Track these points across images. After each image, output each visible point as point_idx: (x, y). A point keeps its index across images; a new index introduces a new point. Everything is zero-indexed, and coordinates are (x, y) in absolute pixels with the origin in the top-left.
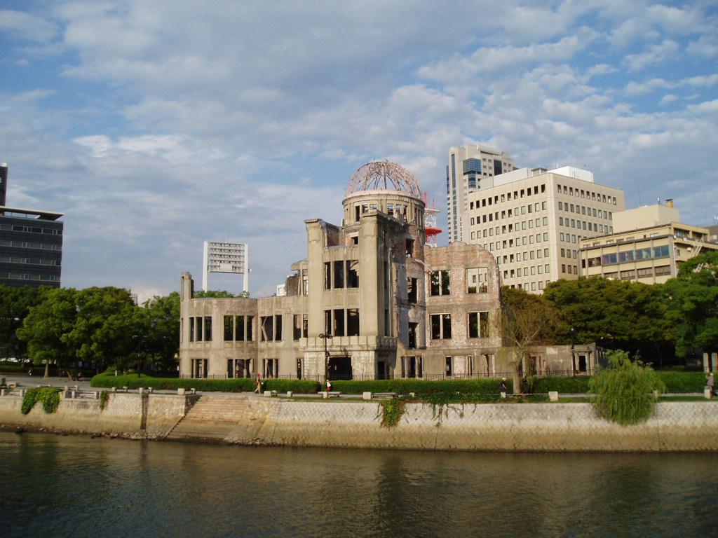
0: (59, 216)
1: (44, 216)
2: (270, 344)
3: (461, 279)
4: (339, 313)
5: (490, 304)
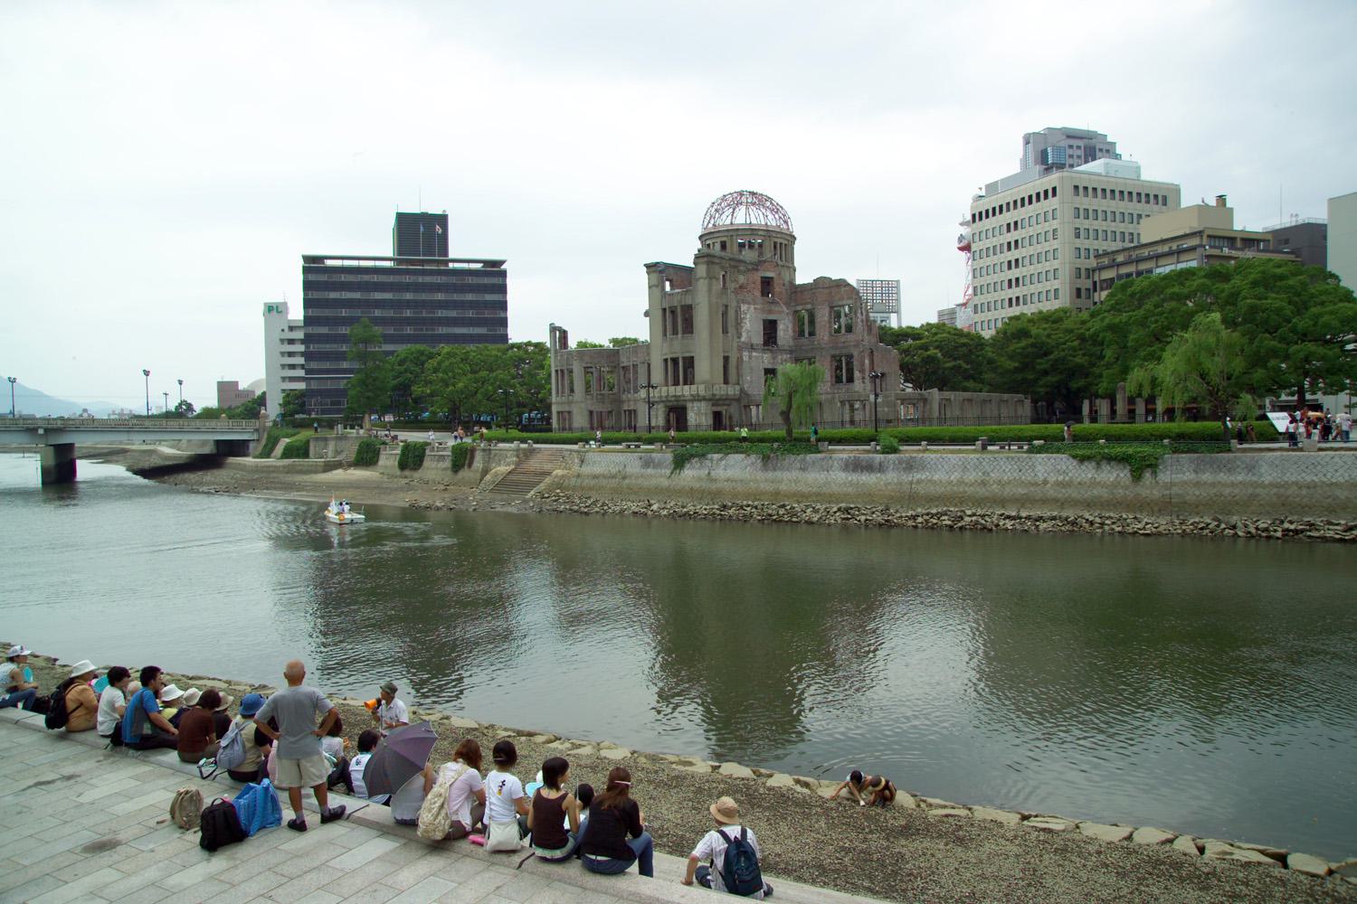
0: (502, 262)
1: (486, 263)
2: (629, 396)
3: (826, 318)
4: (675, 361)
5: (855, 346)
